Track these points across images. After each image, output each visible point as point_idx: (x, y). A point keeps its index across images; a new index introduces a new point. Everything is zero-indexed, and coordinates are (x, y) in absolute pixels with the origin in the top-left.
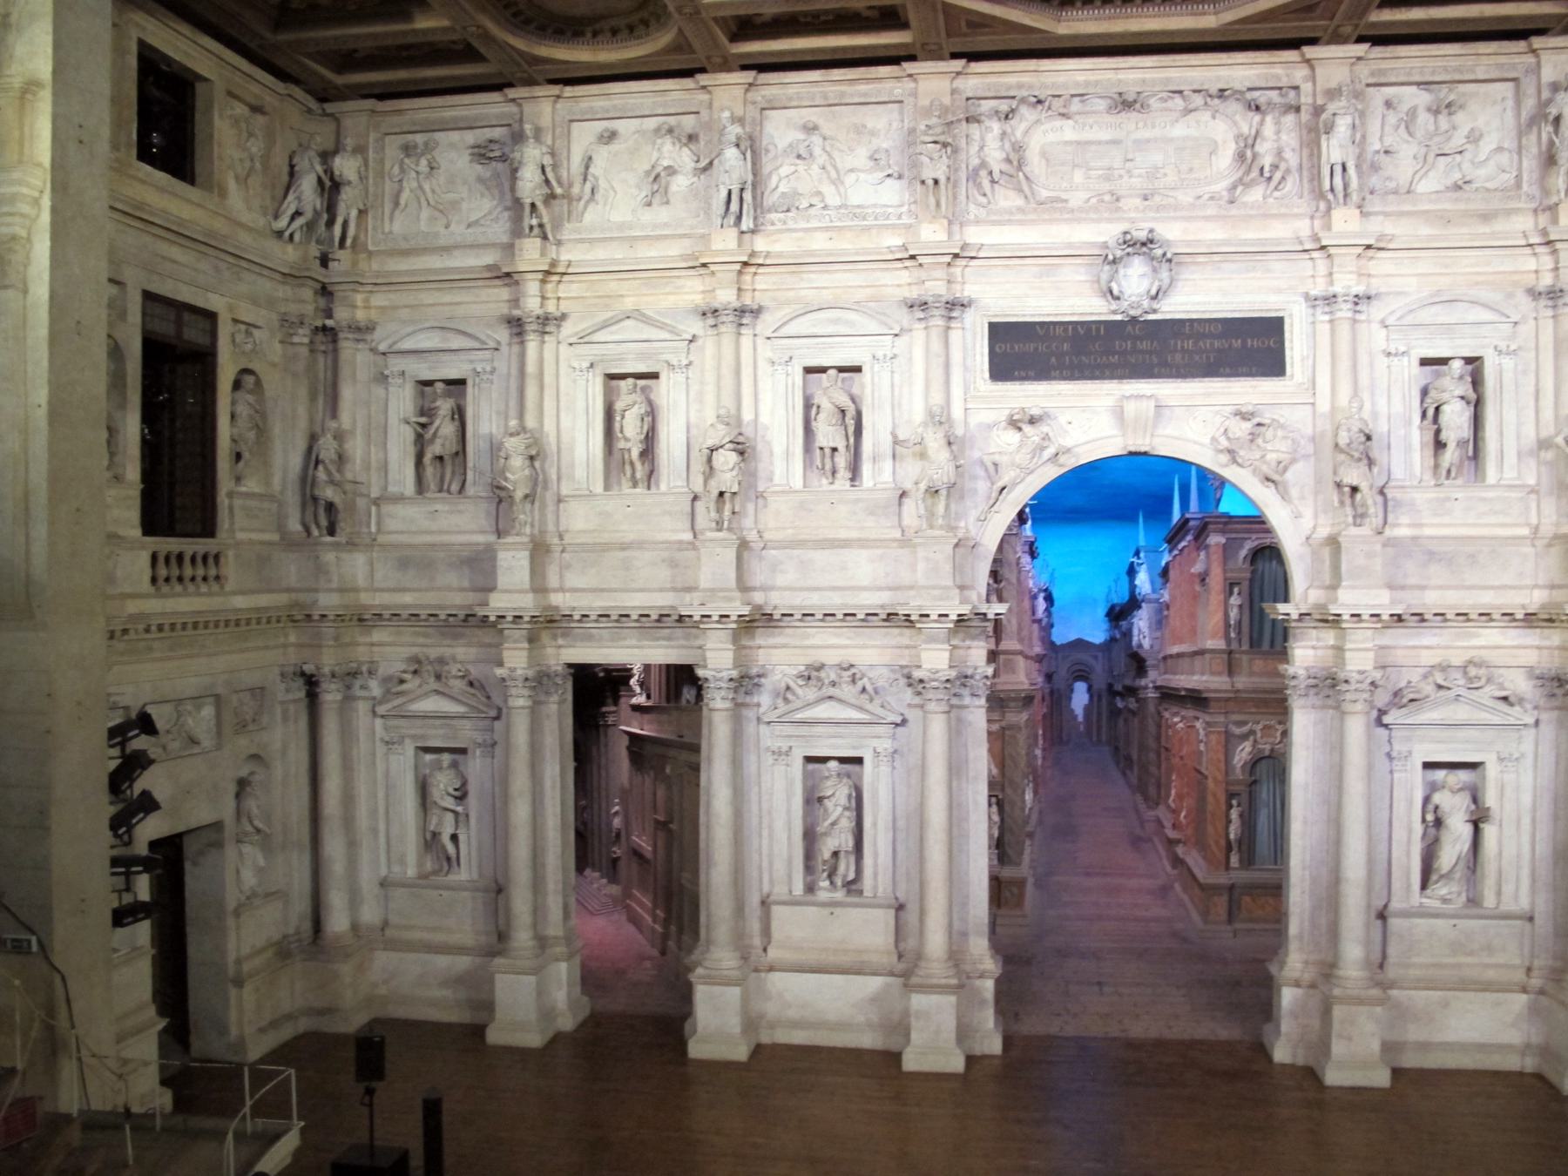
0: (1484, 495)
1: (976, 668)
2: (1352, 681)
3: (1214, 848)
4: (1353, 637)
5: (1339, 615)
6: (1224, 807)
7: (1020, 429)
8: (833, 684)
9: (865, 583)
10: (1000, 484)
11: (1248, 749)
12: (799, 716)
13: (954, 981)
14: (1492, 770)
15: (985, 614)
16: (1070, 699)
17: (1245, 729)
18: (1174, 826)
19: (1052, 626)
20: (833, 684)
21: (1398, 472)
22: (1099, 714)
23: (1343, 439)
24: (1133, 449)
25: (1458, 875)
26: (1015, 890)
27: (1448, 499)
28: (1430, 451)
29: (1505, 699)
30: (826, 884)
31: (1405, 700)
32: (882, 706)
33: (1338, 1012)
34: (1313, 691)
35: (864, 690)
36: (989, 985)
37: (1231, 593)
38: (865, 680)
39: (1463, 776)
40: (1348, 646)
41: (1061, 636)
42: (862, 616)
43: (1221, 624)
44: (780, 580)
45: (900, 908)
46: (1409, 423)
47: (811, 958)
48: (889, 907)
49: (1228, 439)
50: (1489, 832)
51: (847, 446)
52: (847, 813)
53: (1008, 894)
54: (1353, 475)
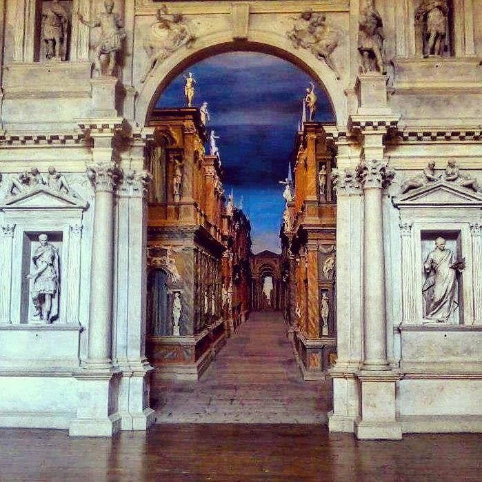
0: (455, 63)
1: (135, 172)
2: (369, 168)
3: (313, 324)
4: (370, 141)
5: (358, 124)
6: (318, 298)
7: (168, 27)
8: (44, 183)
9: (67, 119)
10: (154, 57)
11: (332, 261)
12: (21, 205)
13: (108, 371)
14: (466, 235)
15: (139, 136)
16: (263, 287)
17: (329, 250)
18: (298, 325)
19: (248, 242)
20: (44, 183)
21: (401, 52)
22: (278, 294)
23: (363, 19)
24: (236, 36)
25: (447, 305)
26: (190, 351)
27: (431, 67)
28: (420, 39)
29: (470, 186)
30: (38, 317)
31: (406, 187)
32: (75, 196)
33: (365, 386)
34: (349, 185)
35: (62, 185)
36: (139, 381)
37: (321, 169)
38: (62, 178)
39: (451, 245)
40: (366, 146)
41: (256, 249)
42: (62, 138)
43: (314, 185)
44: (15, 118)
45: (82, 330)
46: (407, 23)
47: (22, 366)
48: (75, 329)
49: (296, 31)
50: (466, 274)
51: (62, 40)
52: (49, 268)
53: (185, 354)
54: (368, 44)
